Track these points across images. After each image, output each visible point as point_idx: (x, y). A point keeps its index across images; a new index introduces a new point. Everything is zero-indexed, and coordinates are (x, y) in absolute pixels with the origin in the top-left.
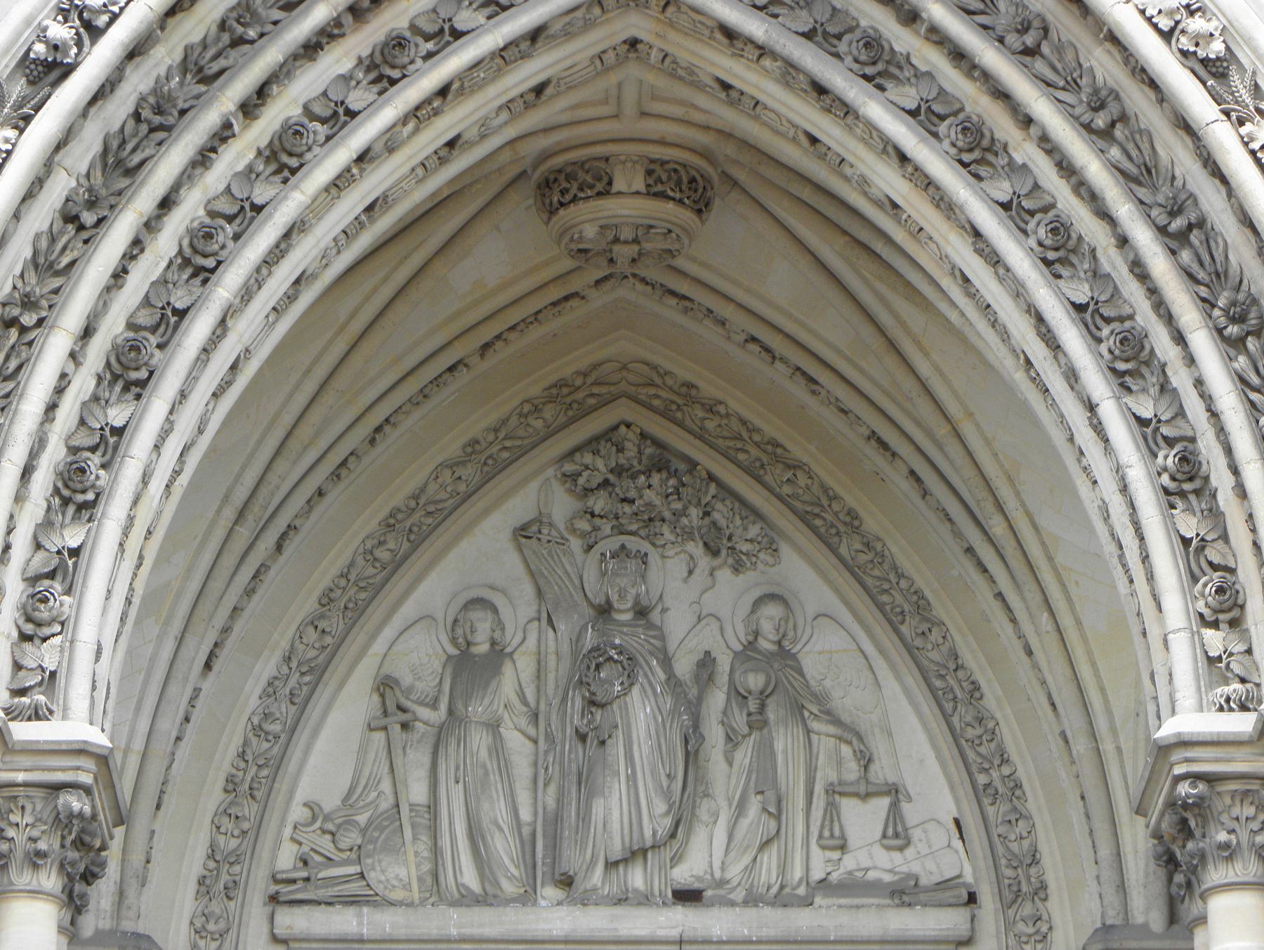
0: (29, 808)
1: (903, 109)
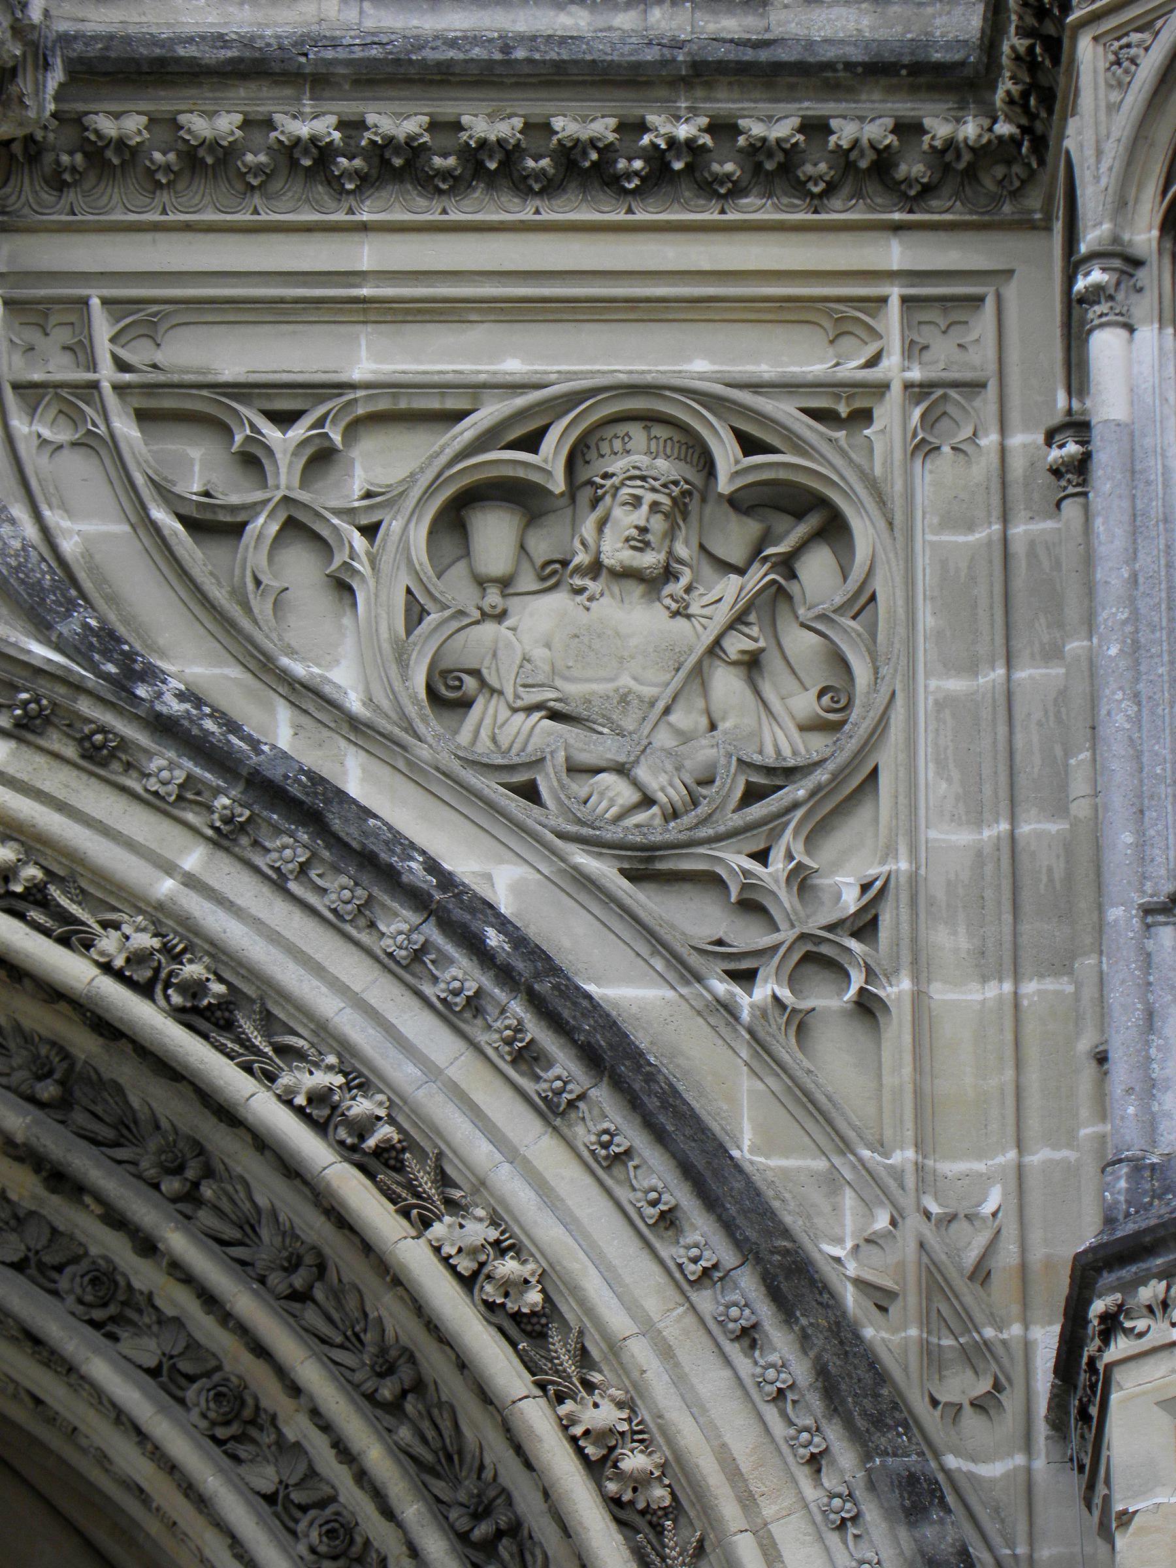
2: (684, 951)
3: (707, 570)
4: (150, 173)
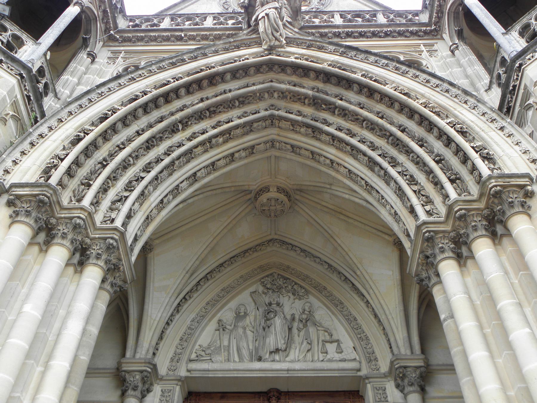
0: (99, 244)
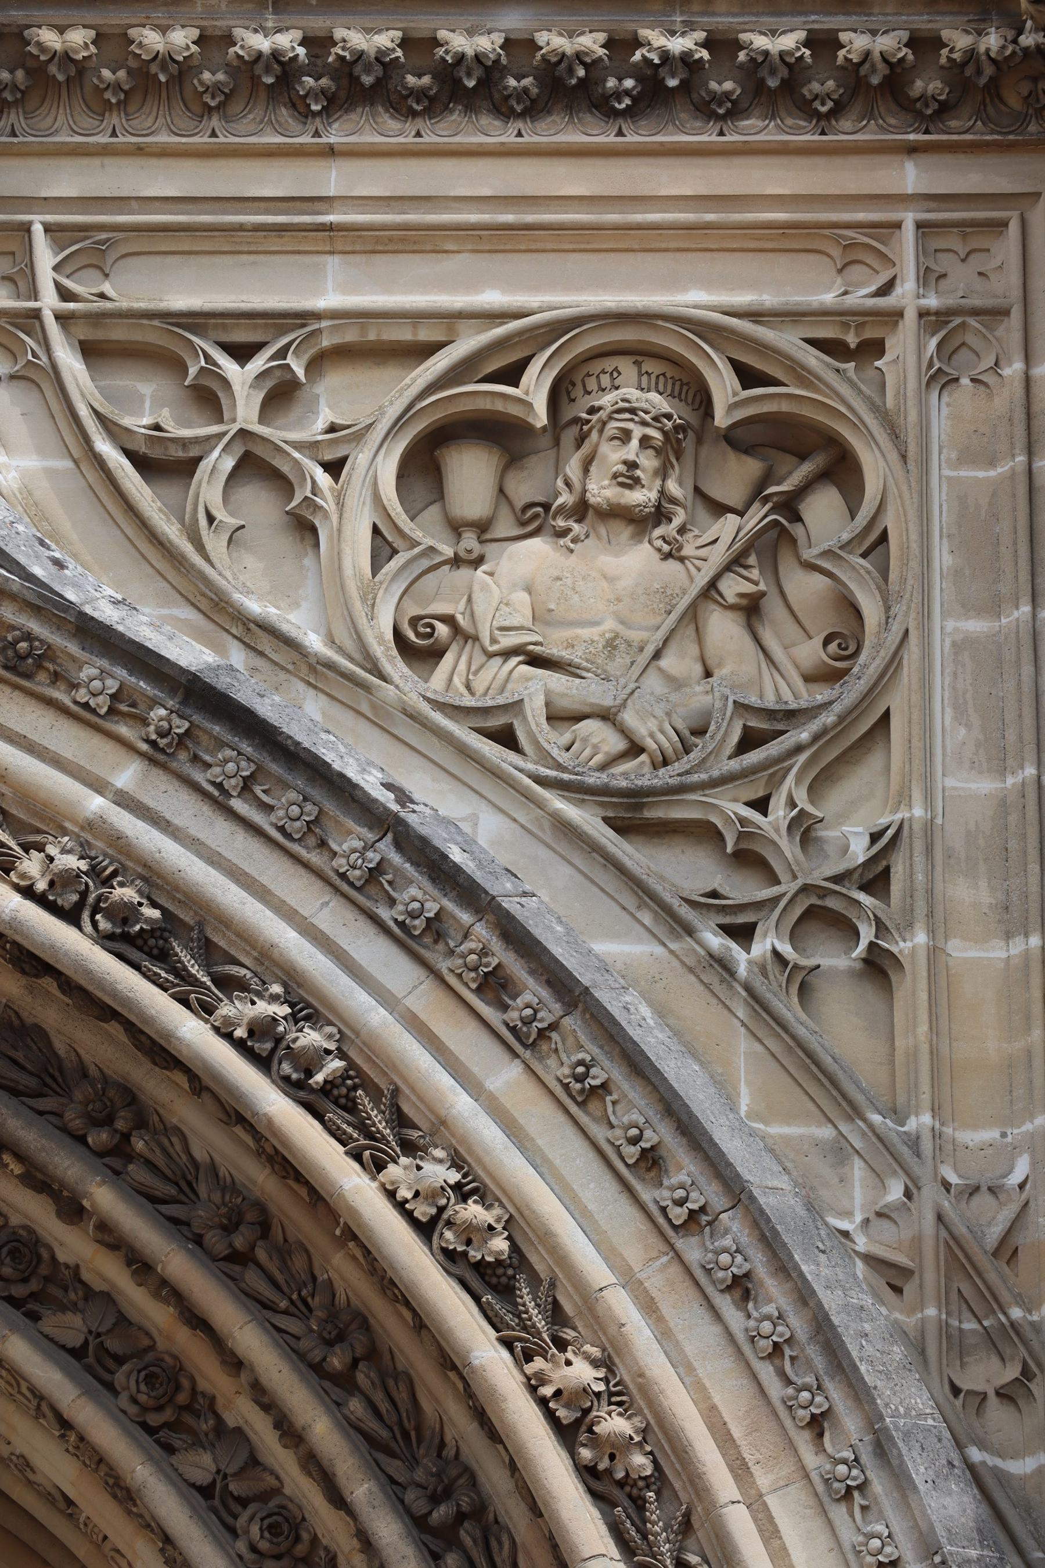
1: (63, 1347)
2: (675, 903)
3: (702, 514)
4: (99, 91)
